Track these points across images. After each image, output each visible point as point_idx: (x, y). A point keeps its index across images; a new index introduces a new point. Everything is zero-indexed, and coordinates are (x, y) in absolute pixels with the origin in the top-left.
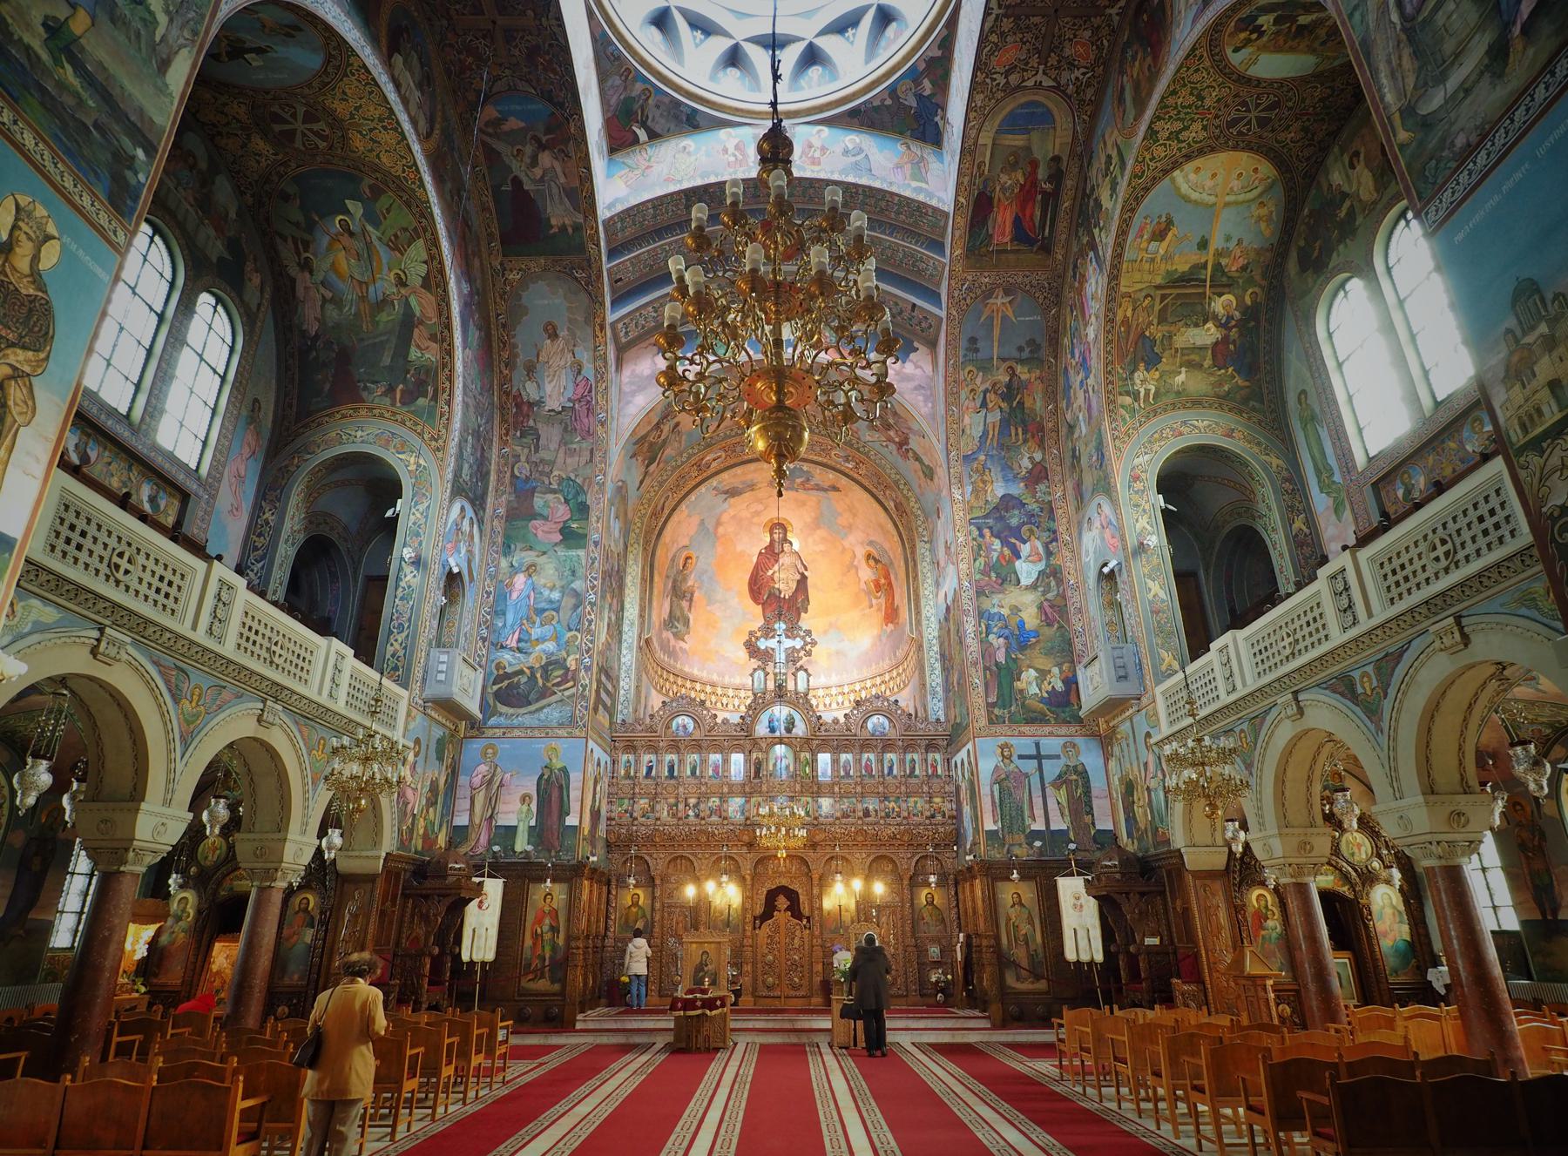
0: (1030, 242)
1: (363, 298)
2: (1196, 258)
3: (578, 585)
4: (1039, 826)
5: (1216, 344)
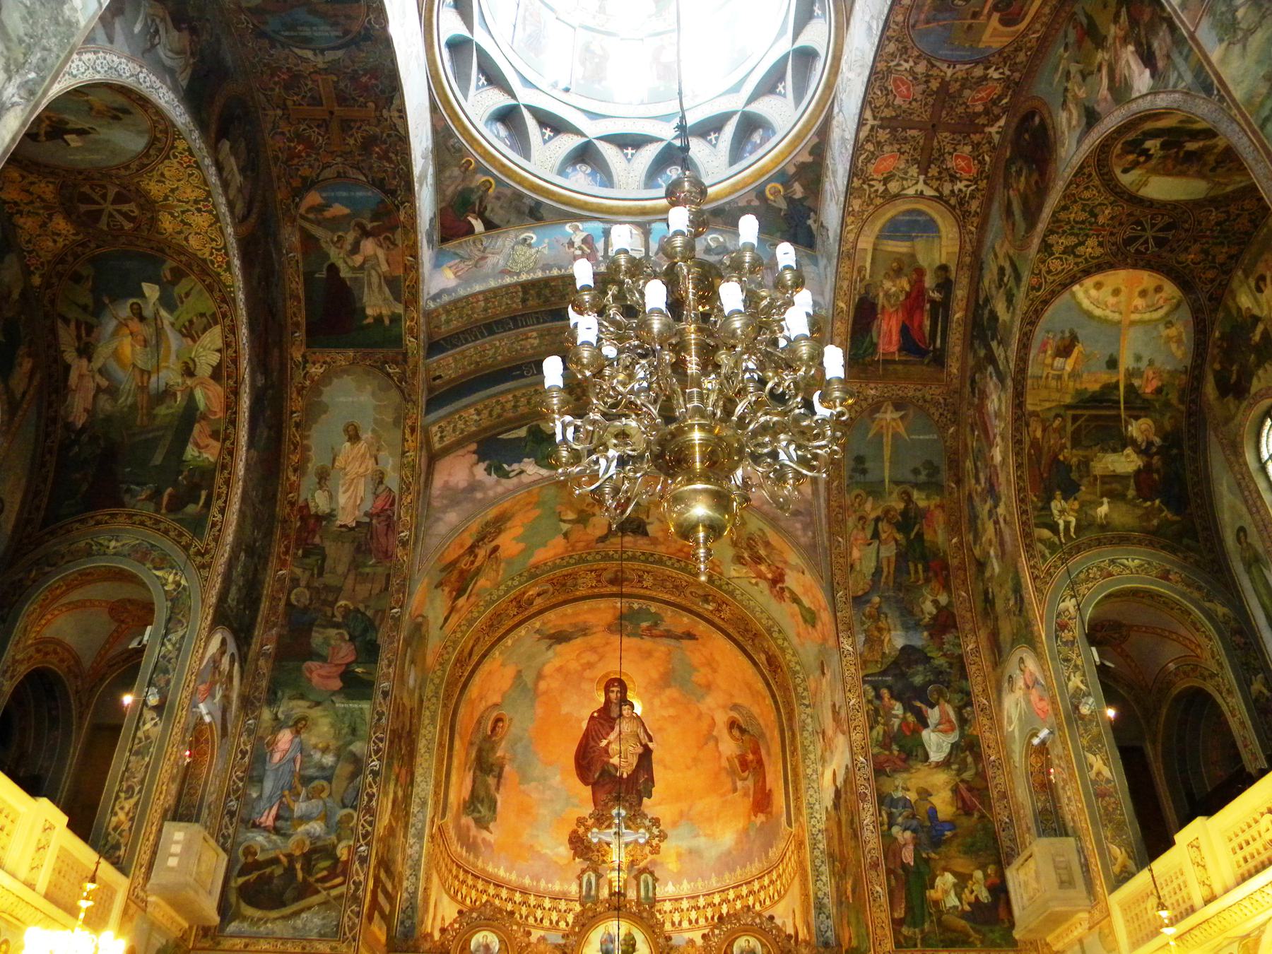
0: (922, 353)
1: (143, 388)
2: (1106, 377)
3: (358, 747)
5: (1138, 472)
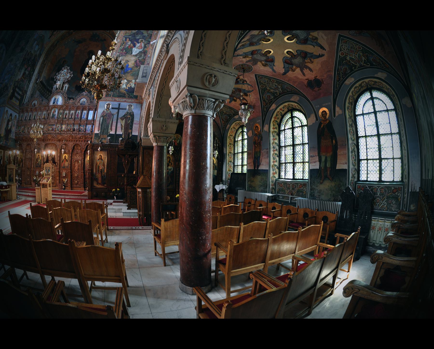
4: (113, 132)
